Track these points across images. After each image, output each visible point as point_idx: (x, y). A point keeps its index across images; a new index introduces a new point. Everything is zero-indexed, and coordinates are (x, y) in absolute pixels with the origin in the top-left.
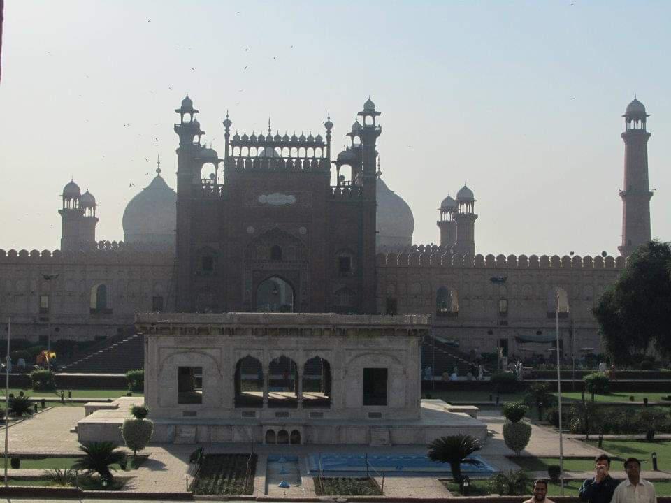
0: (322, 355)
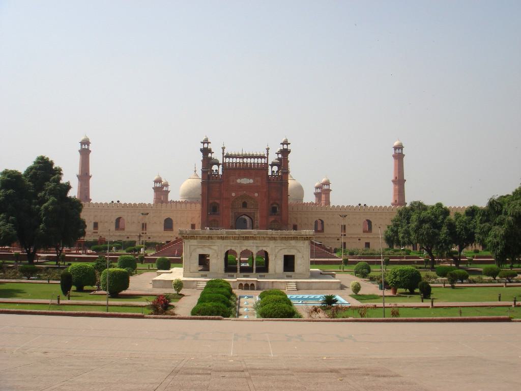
0: (264, 249)
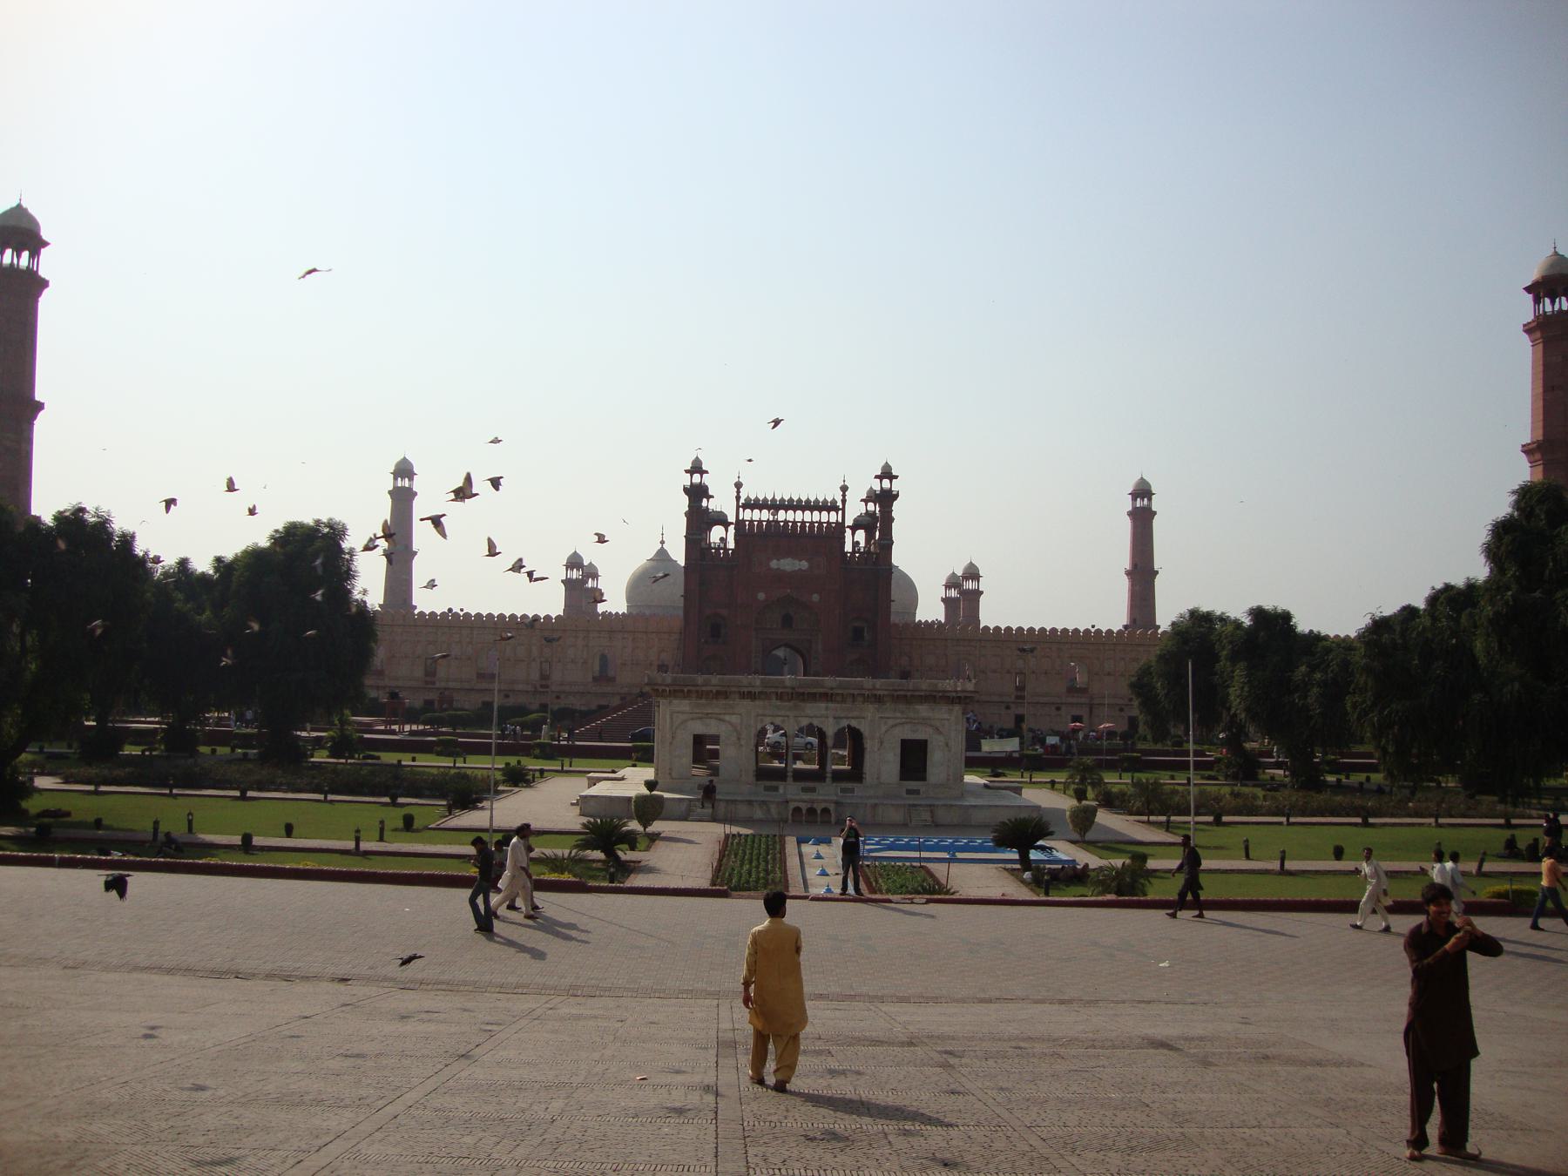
0: (854, 723)
